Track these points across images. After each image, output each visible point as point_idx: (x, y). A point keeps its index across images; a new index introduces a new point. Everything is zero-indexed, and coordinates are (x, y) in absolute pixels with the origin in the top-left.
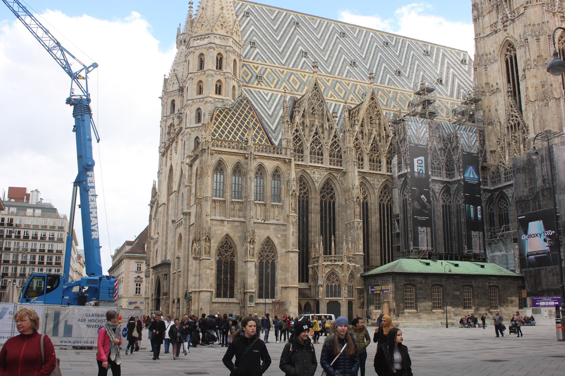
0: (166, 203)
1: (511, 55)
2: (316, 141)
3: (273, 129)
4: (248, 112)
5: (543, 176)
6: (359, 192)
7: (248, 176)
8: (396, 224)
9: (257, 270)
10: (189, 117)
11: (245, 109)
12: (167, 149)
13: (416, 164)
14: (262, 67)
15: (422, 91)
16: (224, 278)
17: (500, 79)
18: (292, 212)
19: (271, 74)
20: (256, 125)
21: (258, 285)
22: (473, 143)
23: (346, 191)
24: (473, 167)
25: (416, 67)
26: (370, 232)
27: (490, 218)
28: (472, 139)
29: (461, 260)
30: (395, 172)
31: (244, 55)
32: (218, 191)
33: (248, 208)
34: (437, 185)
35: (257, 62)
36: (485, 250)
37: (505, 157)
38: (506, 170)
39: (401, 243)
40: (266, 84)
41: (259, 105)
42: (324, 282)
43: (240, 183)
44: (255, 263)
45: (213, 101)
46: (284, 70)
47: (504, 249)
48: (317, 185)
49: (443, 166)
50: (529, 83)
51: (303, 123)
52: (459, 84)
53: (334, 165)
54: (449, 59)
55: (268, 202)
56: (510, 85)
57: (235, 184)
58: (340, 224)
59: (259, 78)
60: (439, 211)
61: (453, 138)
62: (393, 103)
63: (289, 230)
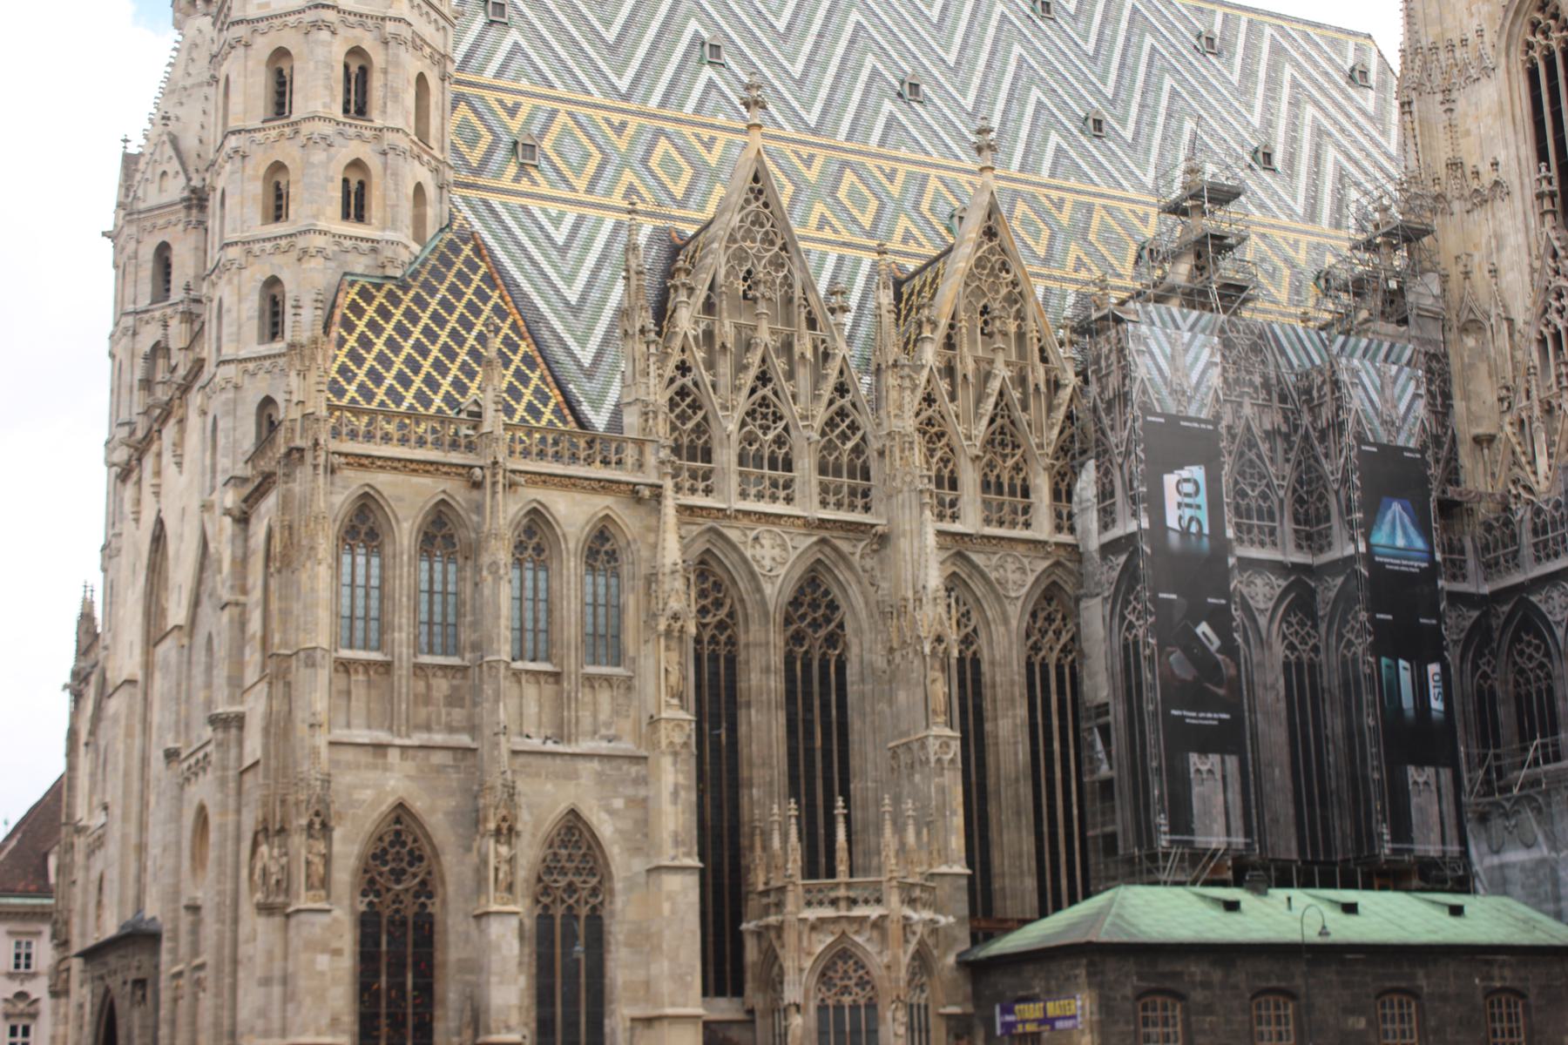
1: (1548, 47)
2: (763, 411)
3: (587, 362)
4: (478, 292)
6: (945, 616)
7: (486, 559)
8: (1099, 746)
9: (527, 950)
10: (234, 314)
11: (468, 282)
12: (140, 448)
13: (1171, 498)
14: (537, 108)
15: (1192, 197)
16: (389, 989)
17: (1506, 146)
18: (668, 705)
19: (571, 134)
20: (514, 348)
21: (533, 1014)
22: (1402, 408)
23: (891, 612)
24: (1408, 503)
25: (1164, 102)
26: (991, 782)
27: (1481, 710)
28: (1397, 391)
29: (1368, 886)
30: (1086, 532)
31: (458, 57)
32: (359, 624)
33: (488, 690)
34: (1259, 581)
35: (515, 86)
36: (1463, 841)
37: (1532, 462)
38: (1538, 512)
39: (1121, 821)
40: (553, 176)
41: (527, 266)
42: (807, 992)
43: (451, 588)
44: (521, 924)
45: (331, 249)
47: (1541, 838)
48: (769, 590)
49: (1281, 502)
51: (709, 335)
52: (1342, 168)
53: (839, 505)
54: (1298, 66)
55: (571, 664)
56: (1548, 169)
57: (431, 592)
58: (869, 748)
59: (524, 151)
60: (1273, 687)
61: (1320, 389)
62: (1075, 250)
63: (659, 780)
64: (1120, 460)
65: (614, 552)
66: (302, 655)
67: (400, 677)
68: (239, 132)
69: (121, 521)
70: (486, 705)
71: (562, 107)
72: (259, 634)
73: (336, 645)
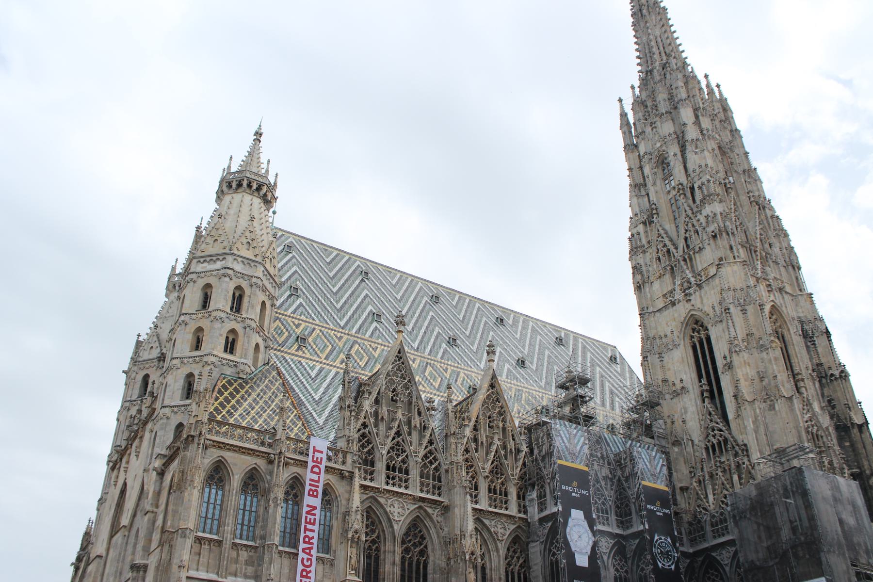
0: (104, 555)
1: (700, 337)
2: (397, 448)
5: (790, 521)
6: (475, 543)
7: (272, 496)
14: (307, 326)
15: (571, 381)
17: (686, 374)
18: (350, 574)
23: (449, 542)
25: (546, 359)
32: (209, 521)
33: (266, 558)
34: (603, 540)
35: (299, 317)
37: (707, 497)
38: (714, 516)
40: (312, 351)
41: (299, 383)
43: (254, 509)
46: (342, 335)
48: (396, 527)
49: (610, 506)
50: (741, 373)
51: (376, 413)
52: (612, 390)
53: (428, 492)
54: (592, 353)
57: (244, 510)
59: (301, 340)
61: (625, 460)
64: (549, 481)
65: (330, 500)
66: (180, 531)
67: (225, 548)
68: (186, 314)
69: (109, 487)
70: (265, 565)
71: (317, 328)
72: (161, 525)
73: (197, 529)
